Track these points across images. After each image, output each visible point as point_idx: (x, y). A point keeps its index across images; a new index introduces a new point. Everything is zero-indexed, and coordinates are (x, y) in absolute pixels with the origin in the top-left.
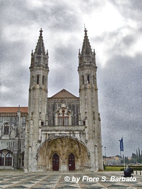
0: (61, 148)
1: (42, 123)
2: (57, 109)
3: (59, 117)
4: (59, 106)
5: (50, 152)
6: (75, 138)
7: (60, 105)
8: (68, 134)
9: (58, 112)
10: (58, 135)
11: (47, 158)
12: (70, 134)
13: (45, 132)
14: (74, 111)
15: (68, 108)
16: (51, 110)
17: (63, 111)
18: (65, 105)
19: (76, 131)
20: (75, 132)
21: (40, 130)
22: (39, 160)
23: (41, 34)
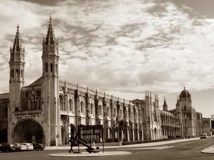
0: (31, 127)
1: (17, 109)
2: (29, 96)
3: (31, 102)
4: (30, 94)
5: (25, 131)
6: (35, 119)
7: (31, 93)
8: (30, 116)
9: (30, 98)
10: (25, 118)
11: (23, 135)
12: (32, 117)
13: (17, 116)
14: (40, 97)
15: (36, 94)
16: (25, 97)
17: (34, 97)
18: (34, 92)
19: (35, 114)
20: (35, 115)
21: (14, 114)
22: (15, 138)
23: (18, 30)
